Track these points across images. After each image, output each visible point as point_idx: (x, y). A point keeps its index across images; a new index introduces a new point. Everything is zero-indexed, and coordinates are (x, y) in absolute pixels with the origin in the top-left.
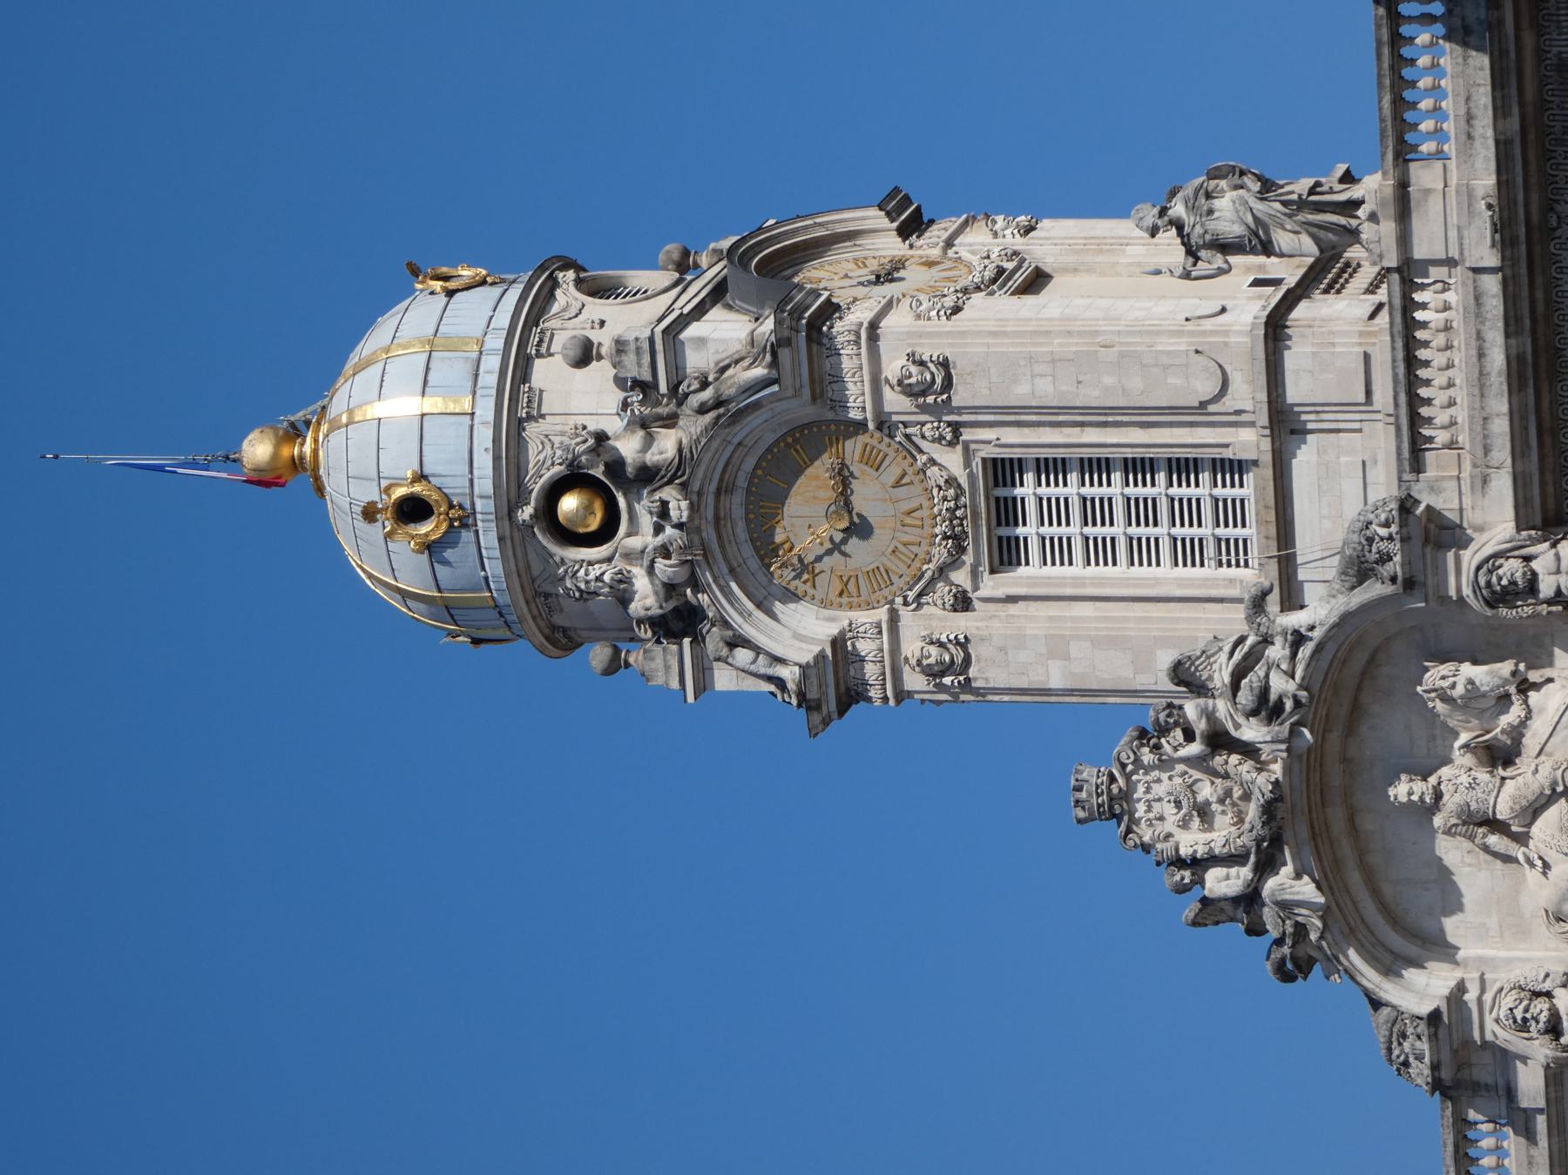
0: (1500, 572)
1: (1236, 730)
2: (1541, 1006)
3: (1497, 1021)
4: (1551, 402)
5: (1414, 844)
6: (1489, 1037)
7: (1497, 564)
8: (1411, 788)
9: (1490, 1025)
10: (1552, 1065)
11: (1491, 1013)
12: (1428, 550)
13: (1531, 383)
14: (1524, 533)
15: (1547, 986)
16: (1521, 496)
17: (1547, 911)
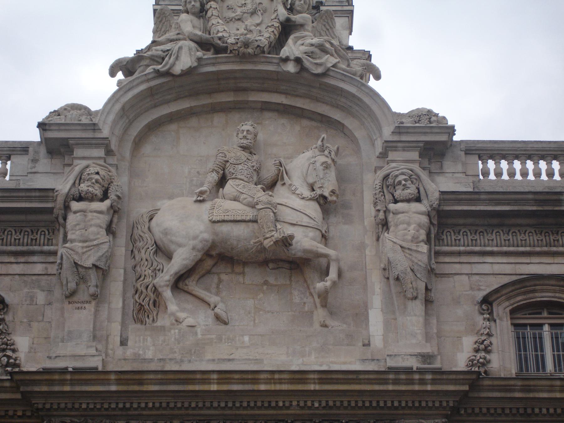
0: (410, 182)
1: (295, 37)
2: (98, 191)
3: (87, 167)
4: (521, 225)
5: (204, 143)
6: (76, 162)
7: (415, 181)
8: (251, 134)
9: (84, 163)
10: (56, 194)
11: (94, 163)
12: (421, 145)
13: (540, 208)
14: (437, 195)
15: (112, 196)
16: (463, 196)
17: (159, 210)
